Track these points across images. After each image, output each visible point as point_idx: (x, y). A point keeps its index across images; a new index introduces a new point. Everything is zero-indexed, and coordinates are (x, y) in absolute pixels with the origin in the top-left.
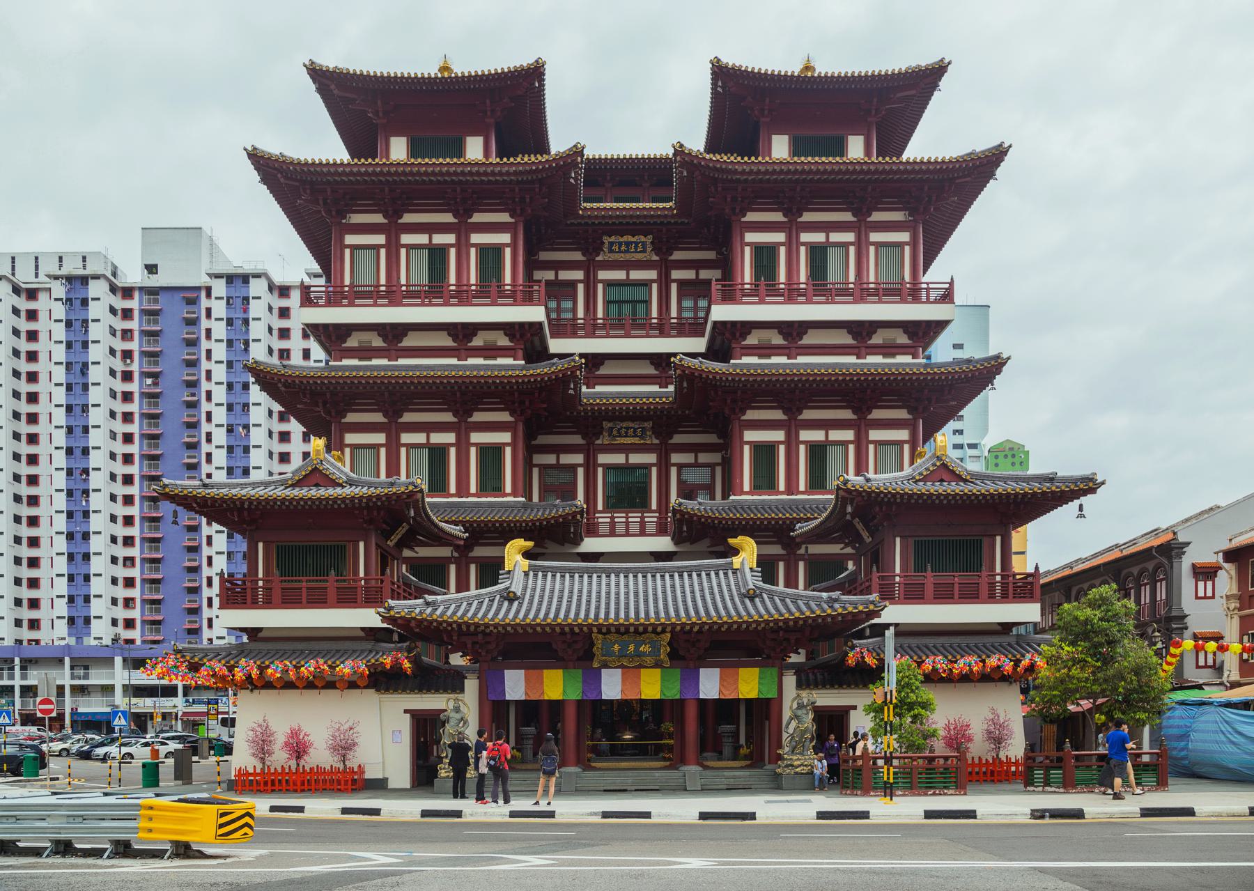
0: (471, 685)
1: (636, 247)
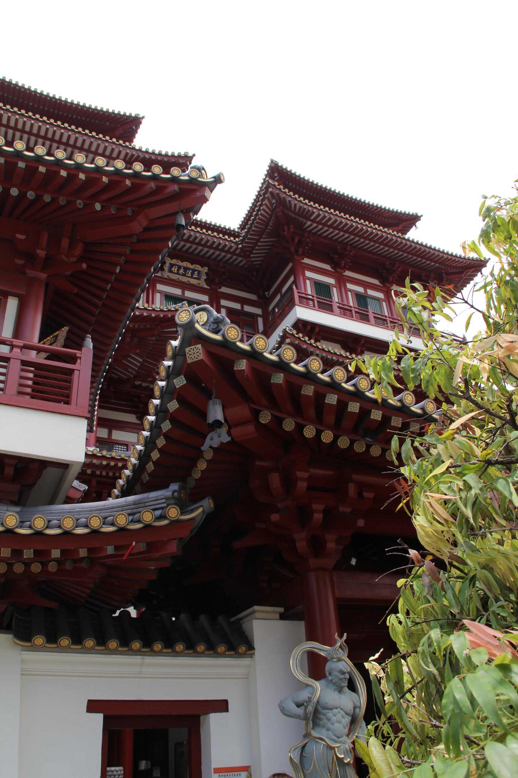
1: (192, 274)
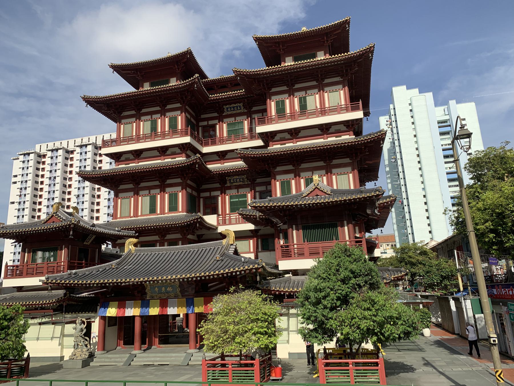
1: (237, 108)
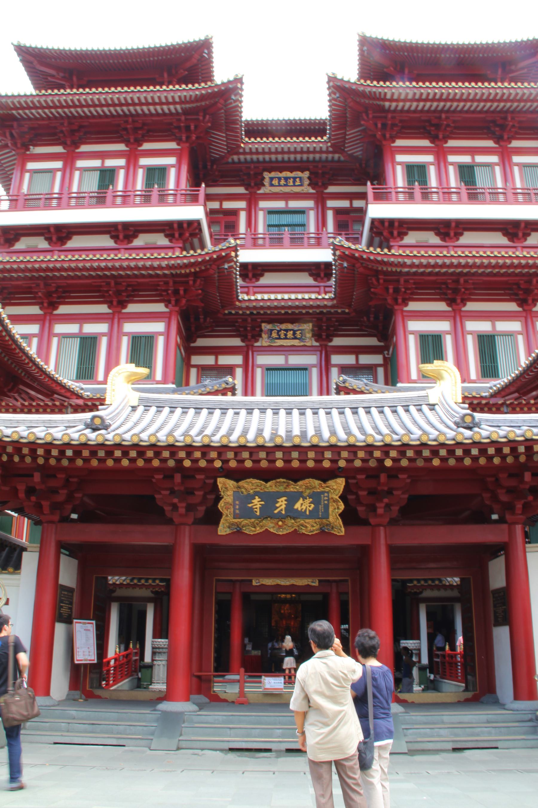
0: (30, 561)
1: (294, 182)
